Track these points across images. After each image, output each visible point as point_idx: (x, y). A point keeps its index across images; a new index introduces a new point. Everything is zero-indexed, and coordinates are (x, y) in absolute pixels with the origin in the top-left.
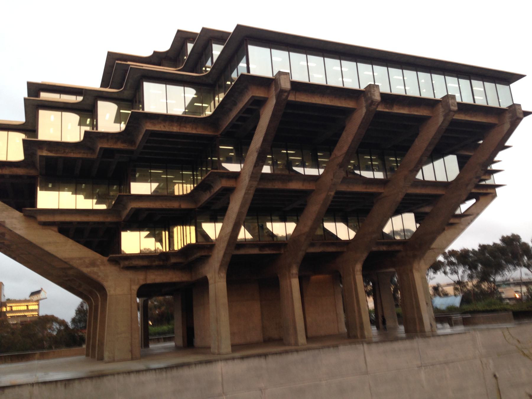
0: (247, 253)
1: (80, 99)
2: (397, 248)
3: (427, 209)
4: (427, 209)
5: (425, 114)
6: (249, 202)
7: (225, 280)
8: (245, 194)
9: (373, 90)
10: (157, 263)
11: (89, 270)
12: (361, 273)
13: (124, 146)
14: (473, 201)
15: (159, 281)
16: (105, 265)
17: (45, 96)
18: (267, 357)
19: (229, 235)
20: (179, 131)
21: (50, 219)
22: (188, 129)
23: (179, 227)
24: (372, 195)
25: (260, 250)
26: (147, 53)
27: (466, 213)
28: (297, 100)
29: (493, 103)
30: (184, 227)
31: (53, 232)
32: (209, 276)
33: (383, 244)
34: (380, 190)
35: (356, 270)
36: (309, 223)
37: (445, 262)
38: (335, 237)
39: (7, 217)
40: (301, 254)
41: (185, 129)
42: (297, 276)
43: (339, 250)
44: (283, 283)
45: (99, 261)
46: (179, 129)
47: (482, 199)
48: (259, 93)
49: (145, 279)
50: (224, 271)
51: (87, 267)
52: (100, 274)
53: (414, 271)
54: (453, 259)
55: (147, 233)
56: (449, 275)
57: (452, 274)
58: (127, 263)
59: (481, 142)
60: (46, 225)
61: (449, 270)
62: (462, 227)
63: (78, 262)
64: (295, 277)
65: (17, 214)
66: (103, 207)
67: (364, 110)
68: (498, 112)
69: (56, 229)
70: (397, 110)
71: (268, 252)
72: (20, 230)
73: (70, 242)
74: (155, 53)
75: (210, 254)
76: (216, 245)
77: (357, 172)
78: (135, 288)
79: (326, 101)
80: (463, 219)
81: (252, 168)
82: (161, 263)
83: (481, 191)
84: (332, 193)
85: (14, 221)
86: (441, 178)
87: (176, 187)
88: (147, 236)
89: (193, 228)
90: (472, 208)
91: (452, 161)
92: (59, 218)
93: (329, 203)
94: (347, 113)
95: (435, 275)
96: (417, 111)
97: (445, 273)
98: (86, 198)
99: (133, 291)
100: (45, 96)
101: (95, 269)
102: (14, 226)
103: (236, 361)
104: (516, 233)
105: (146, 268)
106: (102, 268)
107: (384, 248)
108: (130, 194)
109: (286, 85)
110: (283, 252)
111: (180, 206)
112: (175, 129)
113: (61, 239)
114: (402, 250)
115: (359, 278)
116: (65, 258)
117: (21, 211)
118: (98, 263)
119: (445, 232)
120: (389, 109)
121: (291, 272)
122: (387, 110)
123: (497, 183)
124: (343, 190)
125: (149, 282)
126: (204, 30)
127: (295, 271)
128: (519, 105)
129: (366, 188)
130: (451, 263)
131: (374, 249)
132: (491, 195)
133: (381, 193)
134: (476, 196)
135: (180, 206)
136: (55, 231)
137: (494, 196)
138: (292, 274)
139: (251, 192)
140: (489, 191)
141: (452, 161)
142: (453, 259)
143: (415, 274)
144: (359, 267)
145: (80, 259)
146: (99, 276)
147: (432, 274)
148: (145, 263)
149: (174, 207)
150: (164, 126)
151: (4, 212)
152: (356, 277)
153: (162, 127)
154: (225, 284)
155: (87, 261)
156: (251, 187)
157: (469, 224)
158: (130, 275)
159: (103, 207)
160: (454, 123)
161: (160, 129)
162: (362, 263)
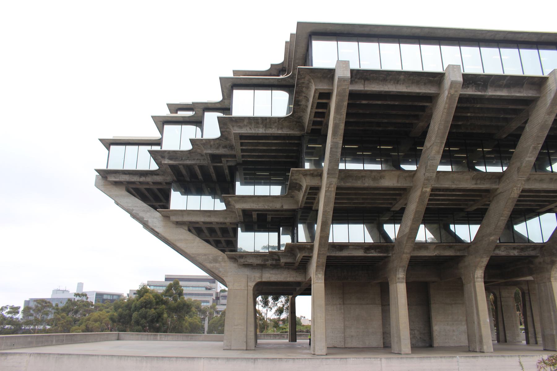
0: (350, 255)
2: (532, 253)
6: (333, 200)
7: (323, 281)
10: (269, 262)
11: (212, 265)
12: (483, 280)
13: (225, 151)
15: (274, 279)
16: (225, 261)
18: (256, 362)
20: (264, 132)
21: (180, 219)
22: (273, 130)
24: (487, 191)
25: (365, 252)
28: (367, 89)
31: (184, 231)
33: (514, 248)
34: (494, 186)
35: (476, 276)
36: (409, 223)
39: (150, 217)
40: (406, 258)
41: (270, 130)
42: (405, 281)
43: (458, 254)
44: (392, 287)
45: (221, 257)
46: (265, 131)
48: (323, 87)
49: (261, 277)
50: (322, 272)
51: (210, 263)
52: (221, 270)
53: (552, 279)
58: (242, 260)
60: (179, 224)
63: (203, 257)
64: (402, 282)
70: (491, 92)
71: (373, 254)
72: (159, 228)
75: (311, 255)
78: (252, 284)
82: (274, 262)
84: (428, 190)
85: (155, 220)
92: (186, 219)
93: (426, 202)
94: (431, 99)
96: (519, 92)
99: (249, 287)
101: (217, 265)
102: (155, 225)
103: (220, 361)
105: (262, 267)
106: (223, 264)
107: (515, 253)
110: (390, 255)
111: (282, 206)
112: (261, 131)
114: (539, 255)
115: (480, 286)
116: (193, 254)
118: (220, 260)
120: (481, 92)
121: (397, 276)
122: (479, 93)
124: (447, 186)
125: (264, 280)
129: (476, 184)
133: (496, 189)
135: (282, 206)
136: (185, 230)
138: (399, 279)
139: (332, 189)
143: (553, 283)
144: (479, 274)
145: (205, 255)
146: (220, 272)
148: (259, 261)
149: (276, 207)
150: (250, 128)
151: (148, 213)
152: (476, 284)
153: (248, 129)
154: (323, 285)
155: (210, 257)
156: (331, 184)
158: (247, 272)
161: (246, 132)
162: (483, 268)
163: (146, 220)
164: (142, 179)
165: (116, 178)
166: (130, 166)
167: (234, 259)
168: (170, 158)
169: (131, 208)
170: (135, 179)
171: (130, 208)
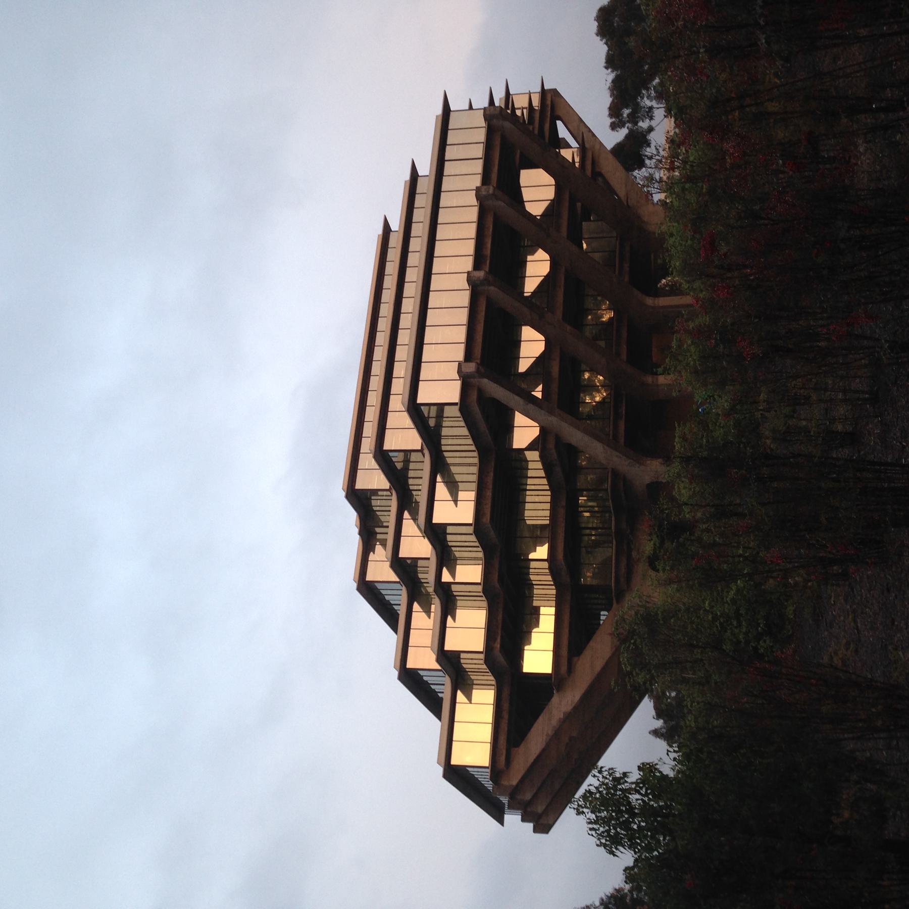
5: (492, 220)
8: (566, 422)
9: (474, 278)
12: (656, 298)
14: (559, 124)
19: (606, 447)
20: (491, 490)
27: (581, 142)
35: (652, 305)
37: (628, 128)
47: (560, 112)
54: (626, 112)
56: (653, 123)
57: (651, 118)
60: (570, 669)
61: (643, 121)
62: (597, 147)
64: (657, 379)
65: (555, 699)
67: (492, 288)
69: (575, 659)
72: (574, 696)
73: (592, 644)
79: (480, 328)
80: (587, 145)
81: (543, 412)
83: (549, 114)
86: (550, 193)
90: (572, 130)
92: (564, 652)
94: (491, 305)
95: (653, 146)
97: (651, 129)
98: (537, 624)
102: (570, 702)
104: (594, 14)
107: (626, 266)
109: (471, 367)
112: (489, 493)
113: (587, 653)
119: (603, 172)
122: (488, 262)
123: (539, 89)
127: (649, 379)
130: (634, 119)
131: (627, 279)
132: (553, 97)
134: (555, 118)
137: (555, 92)
140: (549, 102)
142: (626, 112)
144: (650, 301)
147: (648, 149)
157: (594, 135)
160: (499, 187)
163: (562, 714)
164: (506, 715)
165: (502, 754)
166: (486, 733)
168: (495, 641)
169: (545, 738)
170: (504, 725)
171: (544, 738)
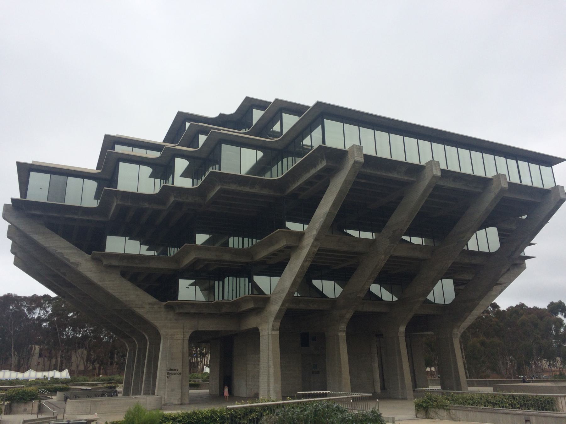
1: (157, 154)
3: (467, 277)
4: (467, 277)
17: (119, 149)
21: (115, 263)
23: (231, 278)
26: (213, 114)
29: (537, 184)
30: (238, 279)
32: (260, 328)
38: (380, 299)
55: (192, 281)
59: (524, 217)
66: (152, 253)
68: (543, 193)
74: (221, 115)
76: (271, 298)
77: (407, 238)
87: (231, 240)
88: (191, 285)
89: (235, 278)
91: (493, 232)
100: (119, 149)
105: (198, 315)
108: (195, 245)
117: (89, 252)
126: (276, 100)
128: (563, 187)
141: (493, 232)
159: (152, 253)
167: (170, 308)
